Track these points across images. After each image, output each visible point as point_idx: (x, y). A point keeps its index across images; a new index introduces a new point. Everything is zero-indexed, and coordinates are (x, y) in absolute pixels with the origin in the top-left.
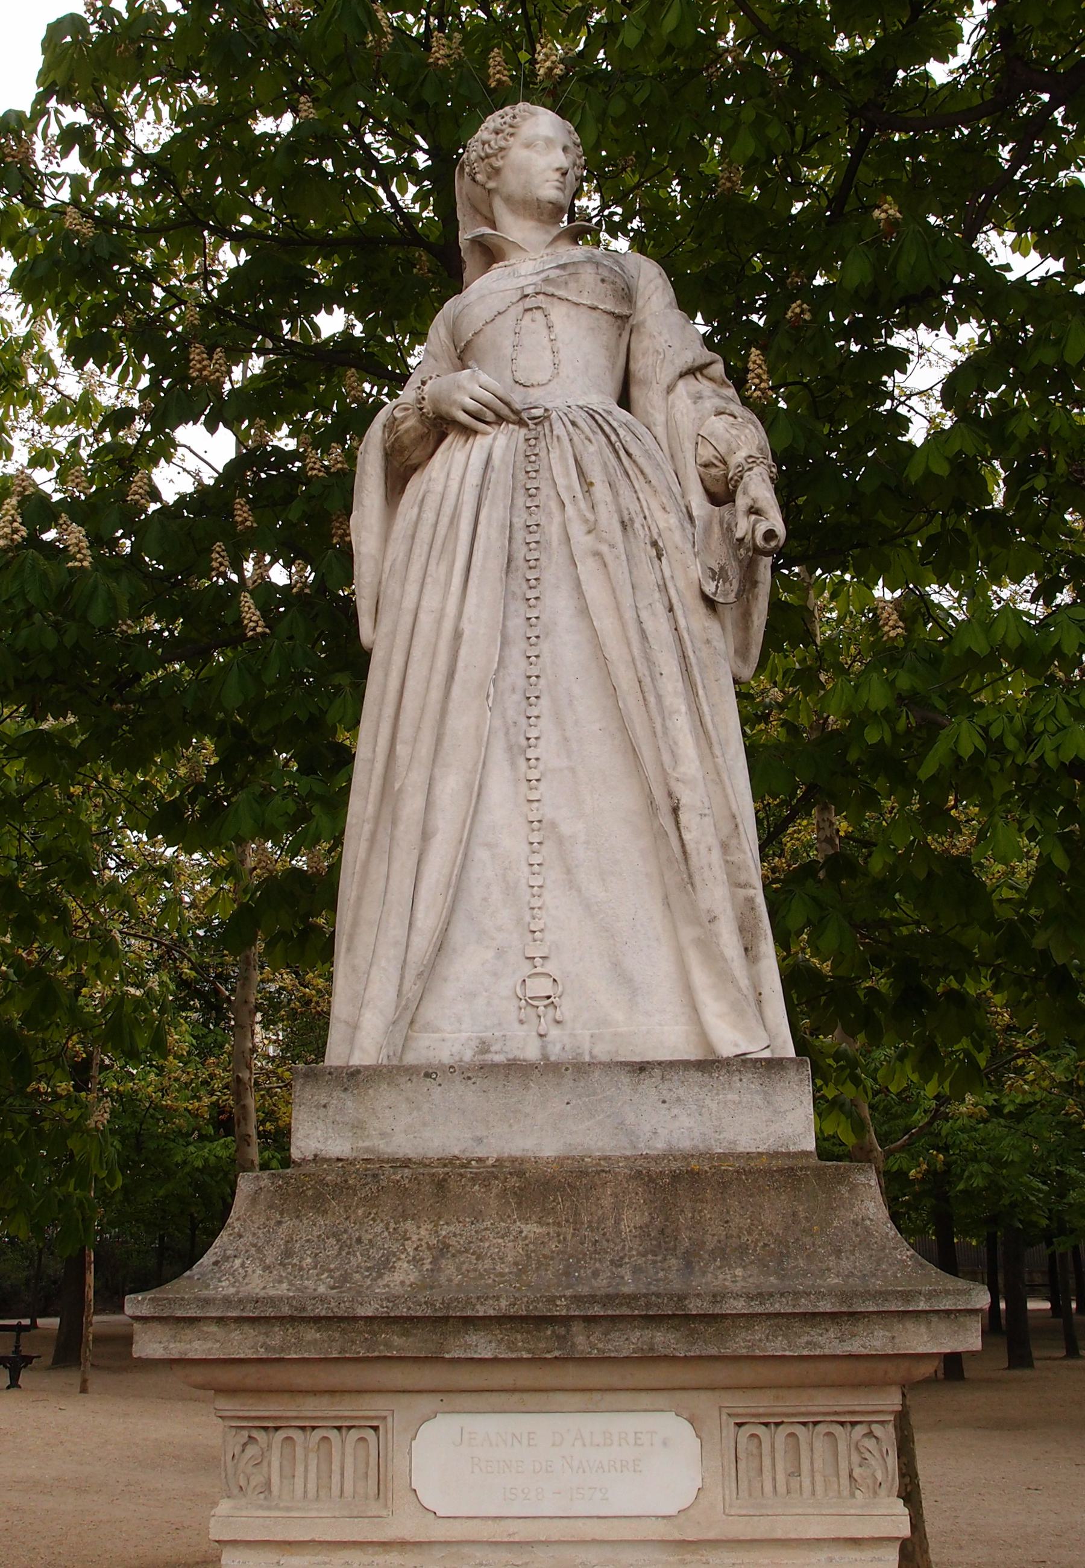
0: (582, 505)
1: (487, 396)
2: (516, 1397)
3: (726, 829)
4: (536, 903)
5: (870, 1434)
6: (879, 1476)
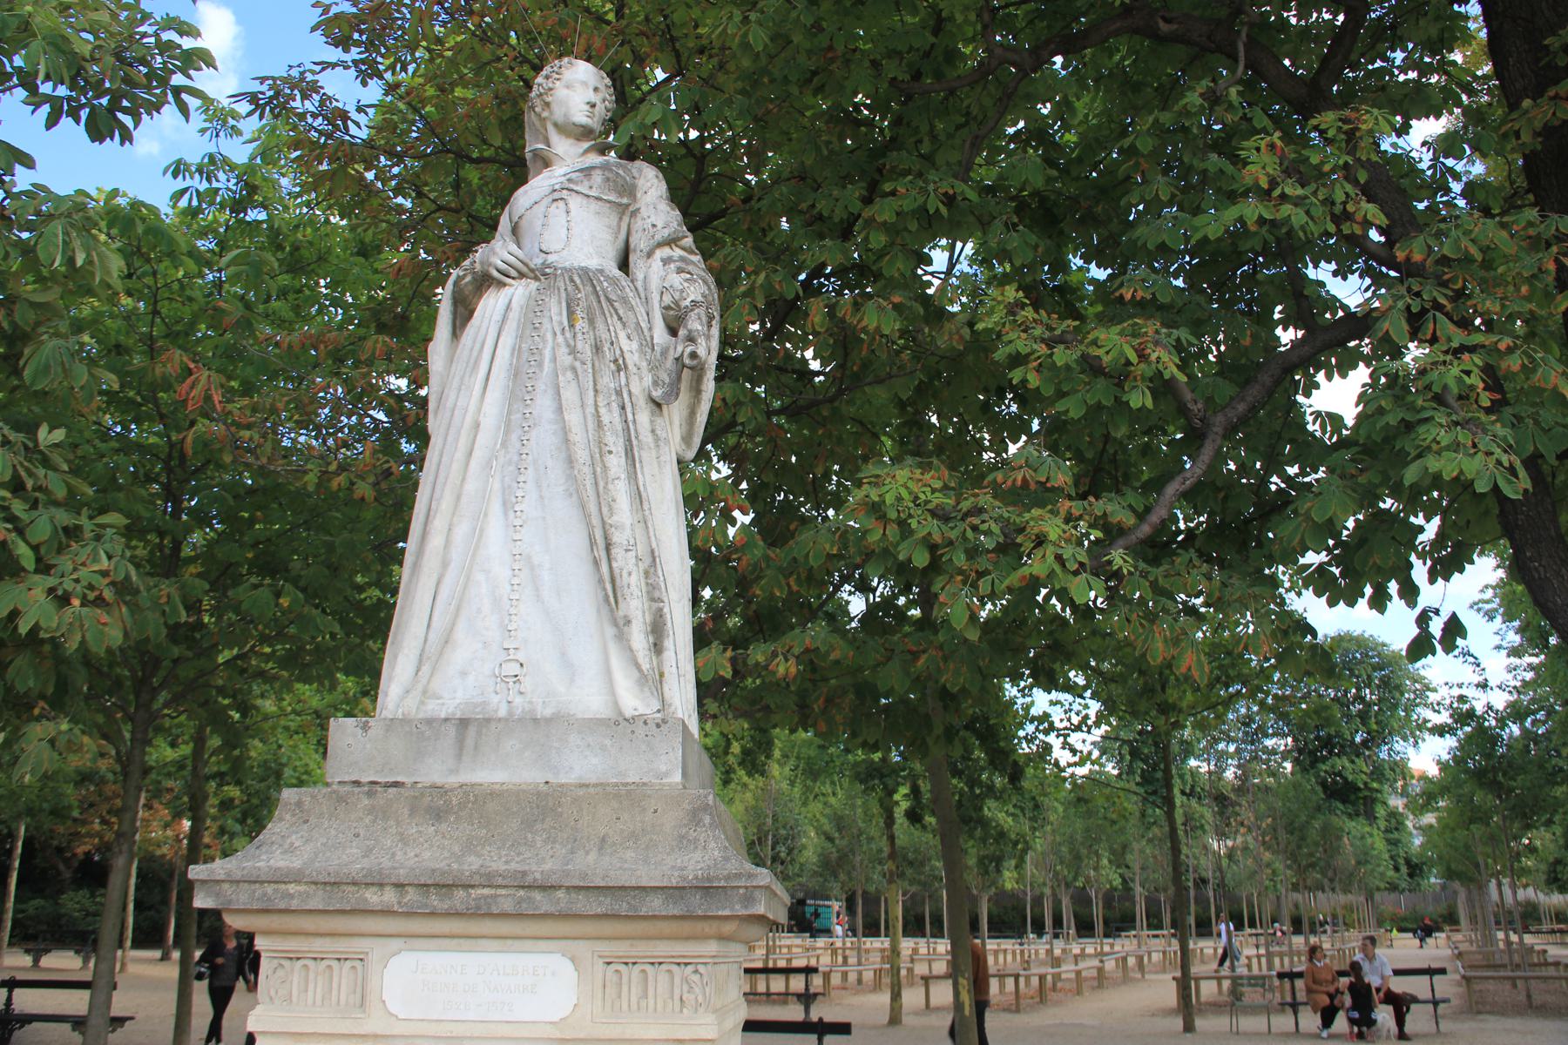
0: (568, 335)
1: (512, 259)
2: (456, 941)
3: (648, 561)
4: (513, 611)
5: (696, 971)
6: (700, 999)
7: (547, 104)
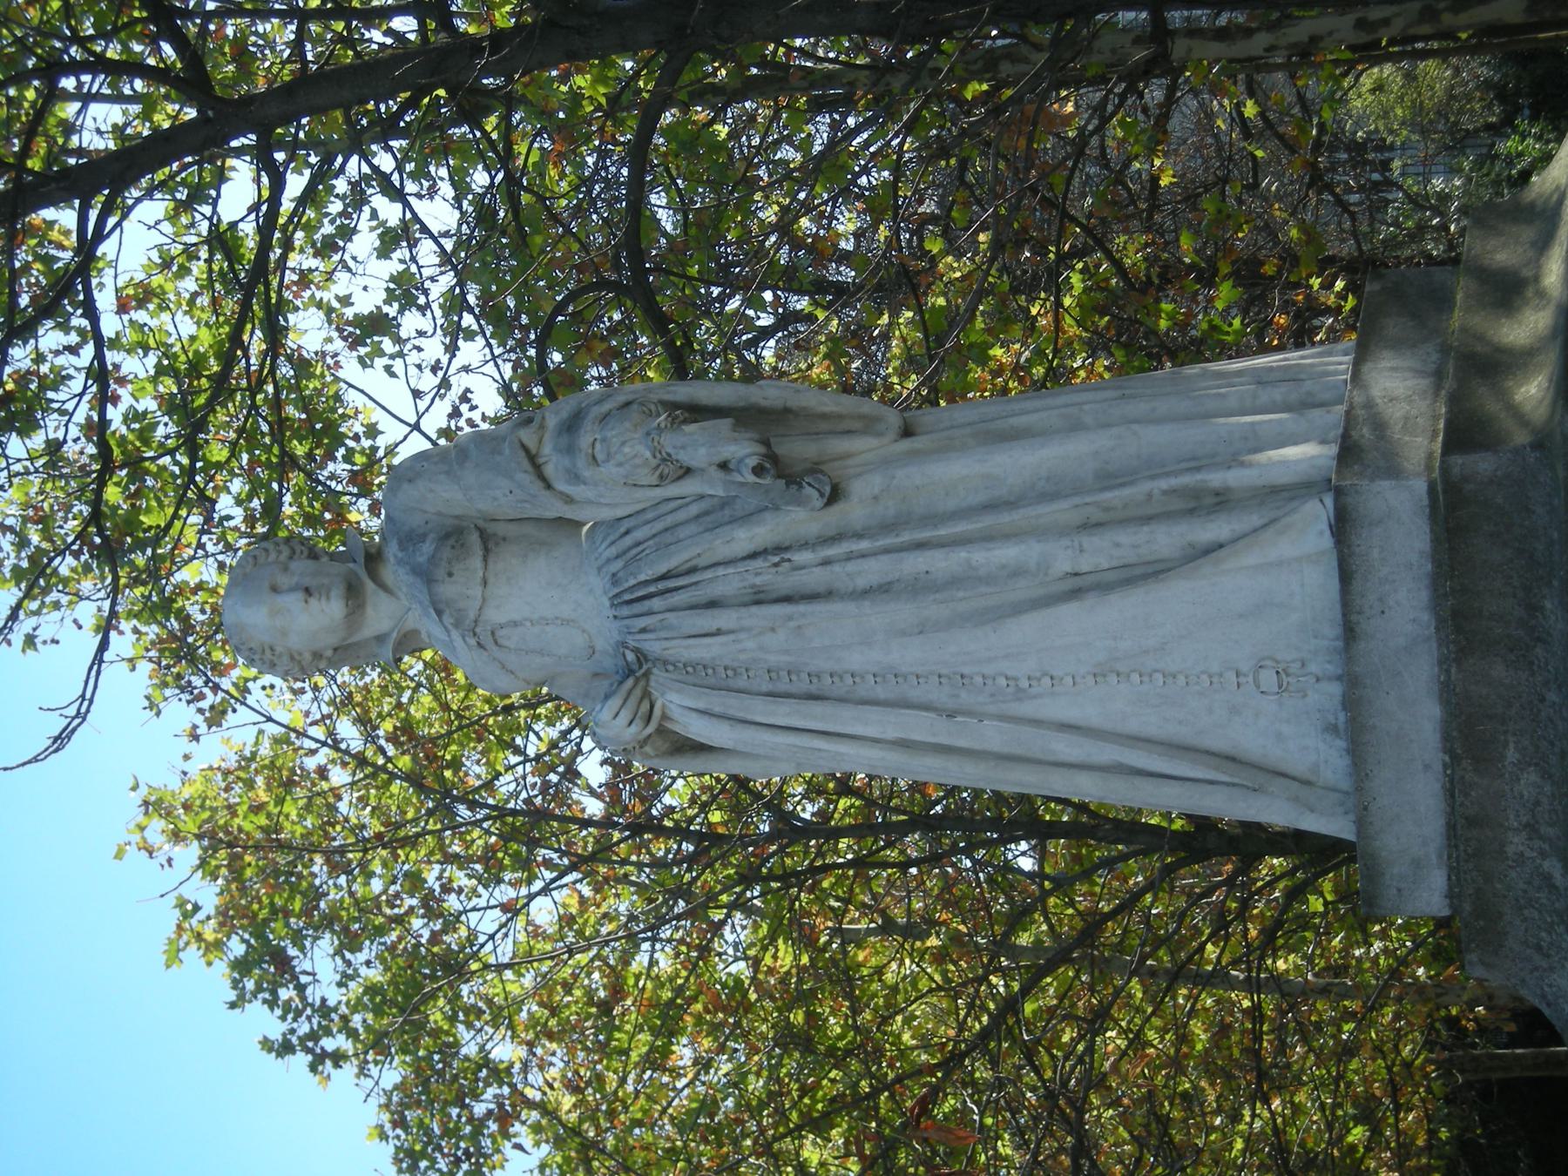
0: (742, 636)
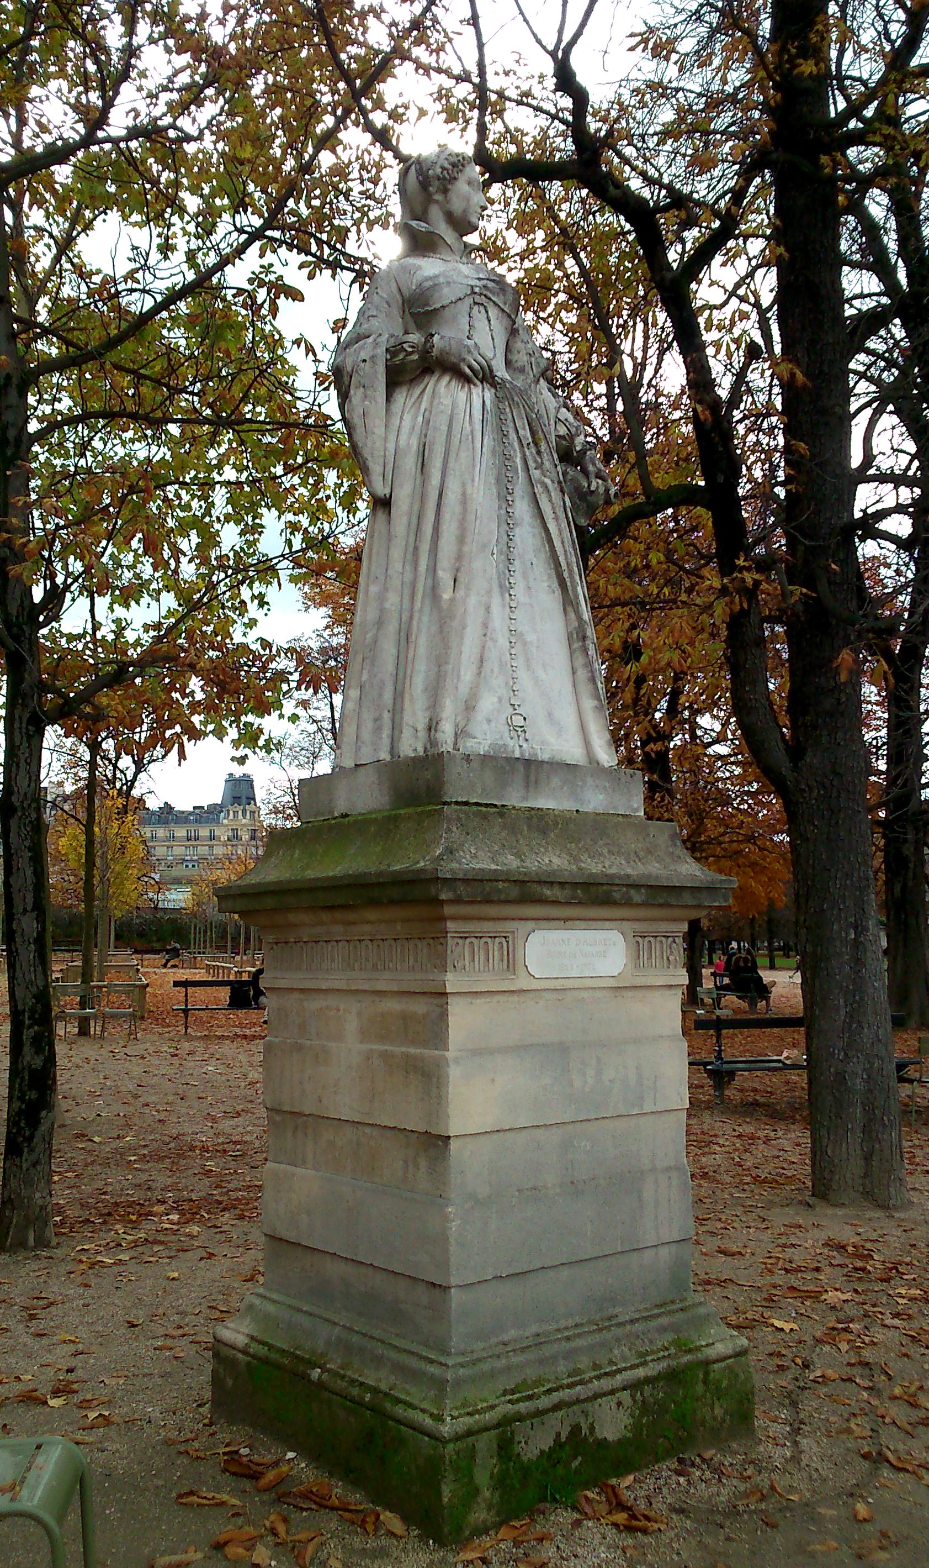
7: (445, 191)
